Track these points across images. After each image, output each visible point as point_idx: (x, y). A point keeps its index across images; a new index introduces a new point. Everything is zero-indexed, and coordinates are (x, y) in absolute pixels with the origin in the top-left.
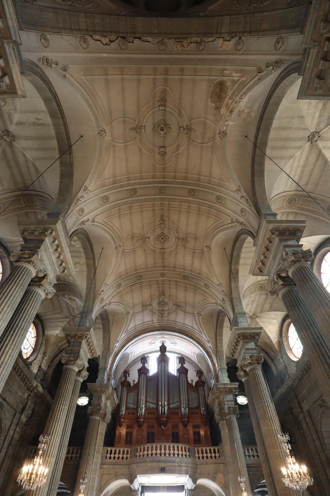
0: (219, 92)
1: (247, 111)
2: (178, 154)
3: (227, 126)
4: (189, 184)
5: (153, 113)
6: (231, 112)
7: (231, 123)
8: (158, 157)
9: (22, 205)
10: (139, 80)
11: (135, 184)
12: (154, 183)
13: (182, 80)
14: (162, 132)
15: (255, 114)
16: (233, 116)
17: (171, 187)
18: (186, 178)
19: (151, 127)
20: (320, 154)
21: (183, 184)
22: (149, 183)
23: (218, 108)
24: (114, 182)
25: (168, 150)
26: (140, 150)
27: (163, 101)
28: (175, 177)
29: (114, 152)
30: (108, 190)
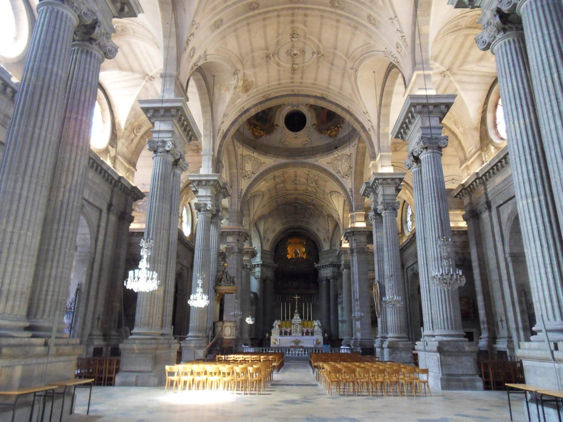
0: (247, 88)
1: (223, 92)
2: (277, 37)
3: (235, 79)
4: (260, 14)
5: (304, 63)
6: (235, 88)
7: (232, 82)
8: (300, 32)
9: (451, 81)
10: (315, 80)
11: (332, 13)
12: (307, 9)
13: (279, 80)
14: (295, 52)
15: (216, 90)
16: (233, 87)
17: (283, 4)
18: (265, 19)
19: (306, 54)
20: (132, 70)
21: (267, 12)
22: (313, 9)
23: (245, 81)
24: (356, 28)
25: (290, 40)
26: (320, 41)
27: (294, 70)
28: (278, 16)
29: (347, 52)
30: (366, 27)
